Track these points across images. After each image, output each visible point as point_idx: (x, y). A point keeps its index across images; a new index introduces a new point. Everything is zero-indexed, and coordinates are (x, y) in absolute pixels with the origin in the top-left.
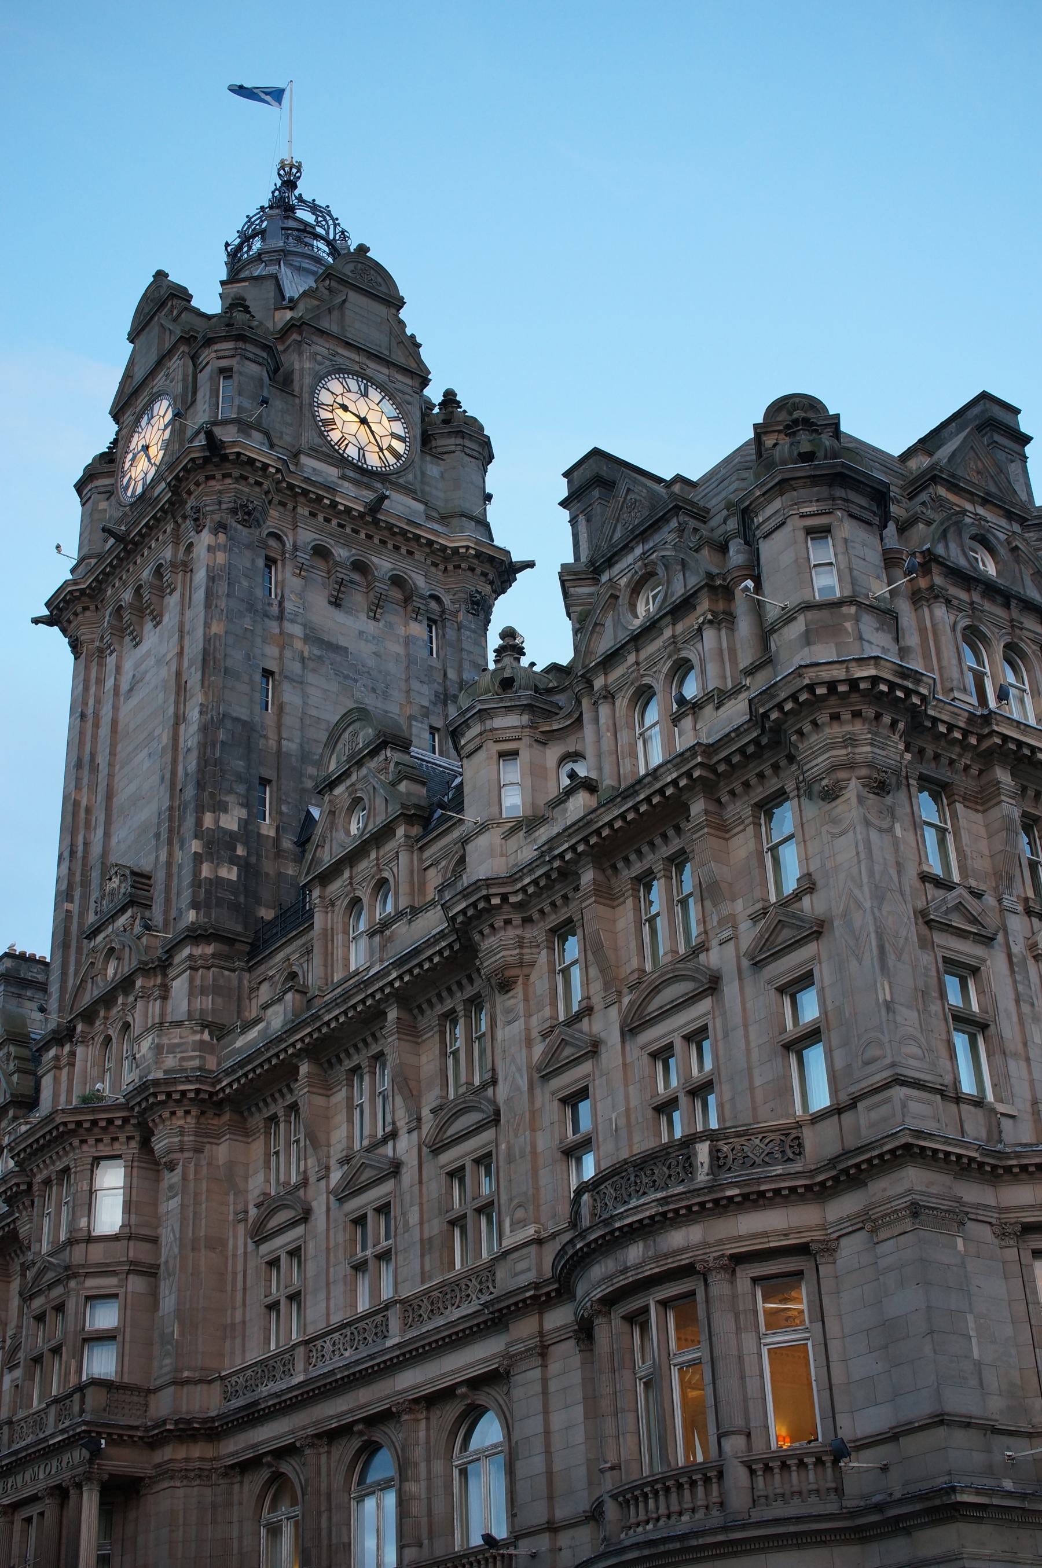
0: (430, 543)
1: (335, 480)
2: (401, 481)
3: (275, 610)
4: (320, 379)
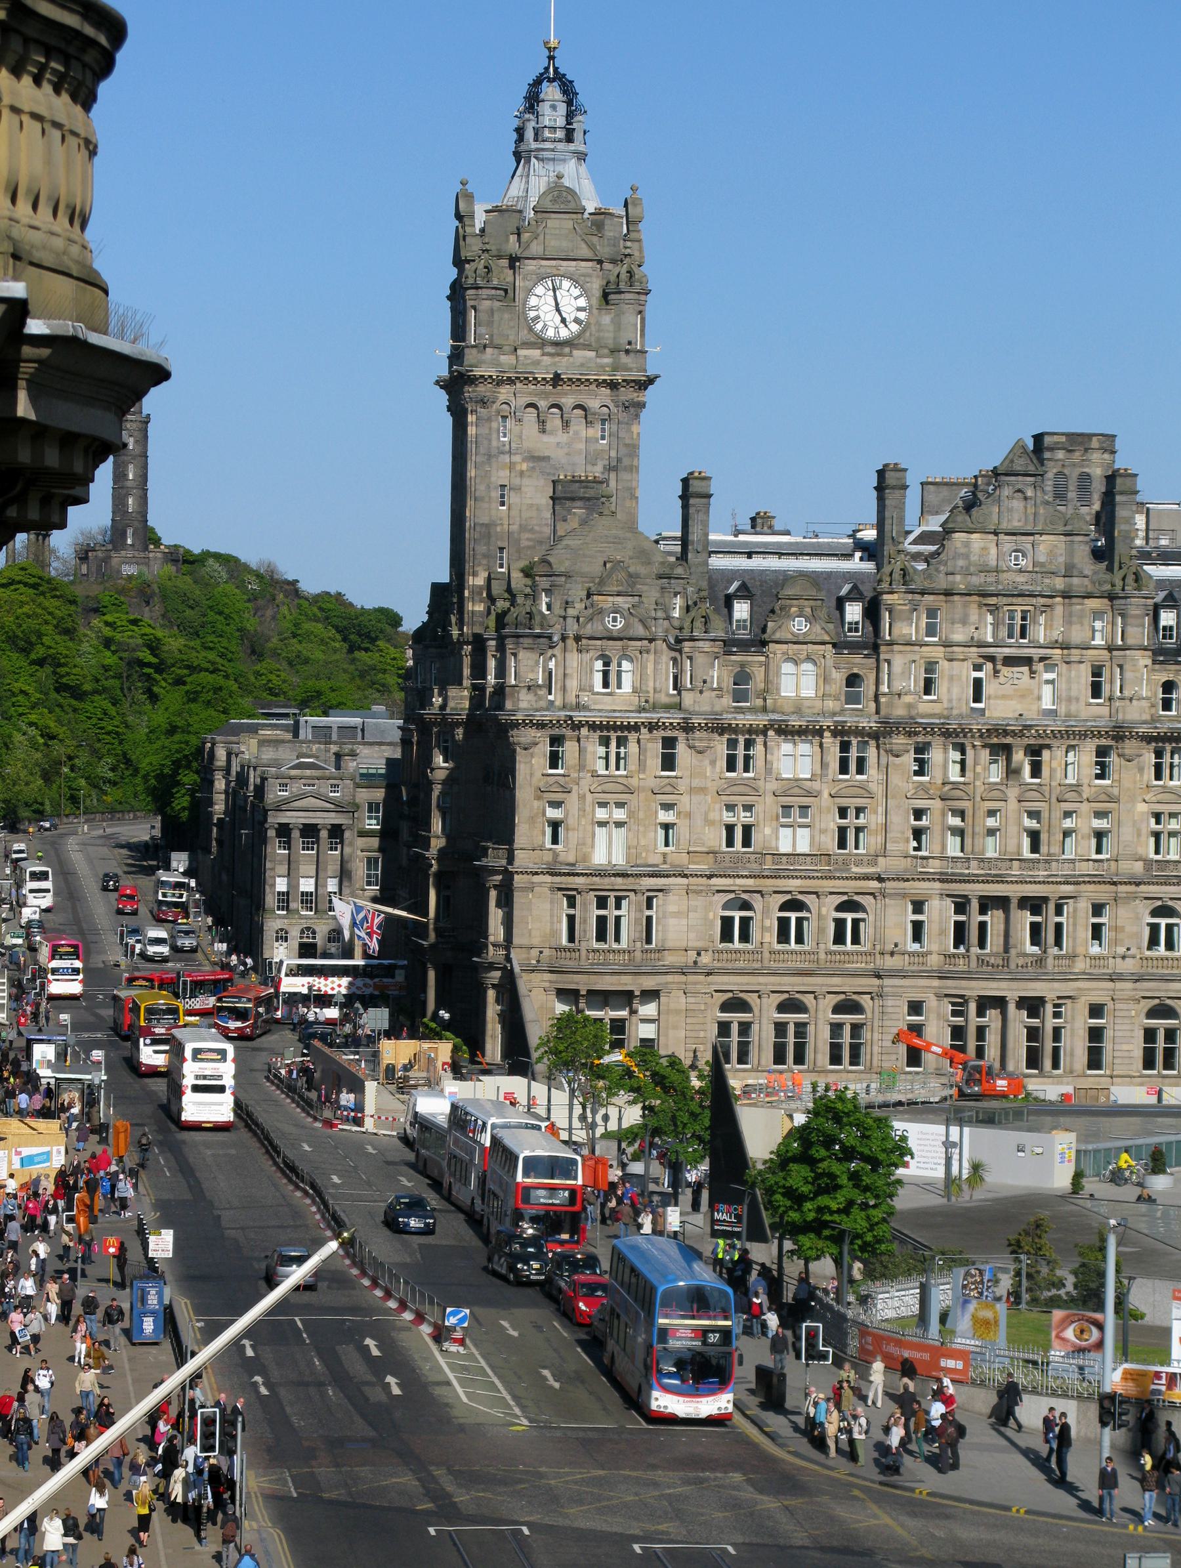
4: (529, 291)
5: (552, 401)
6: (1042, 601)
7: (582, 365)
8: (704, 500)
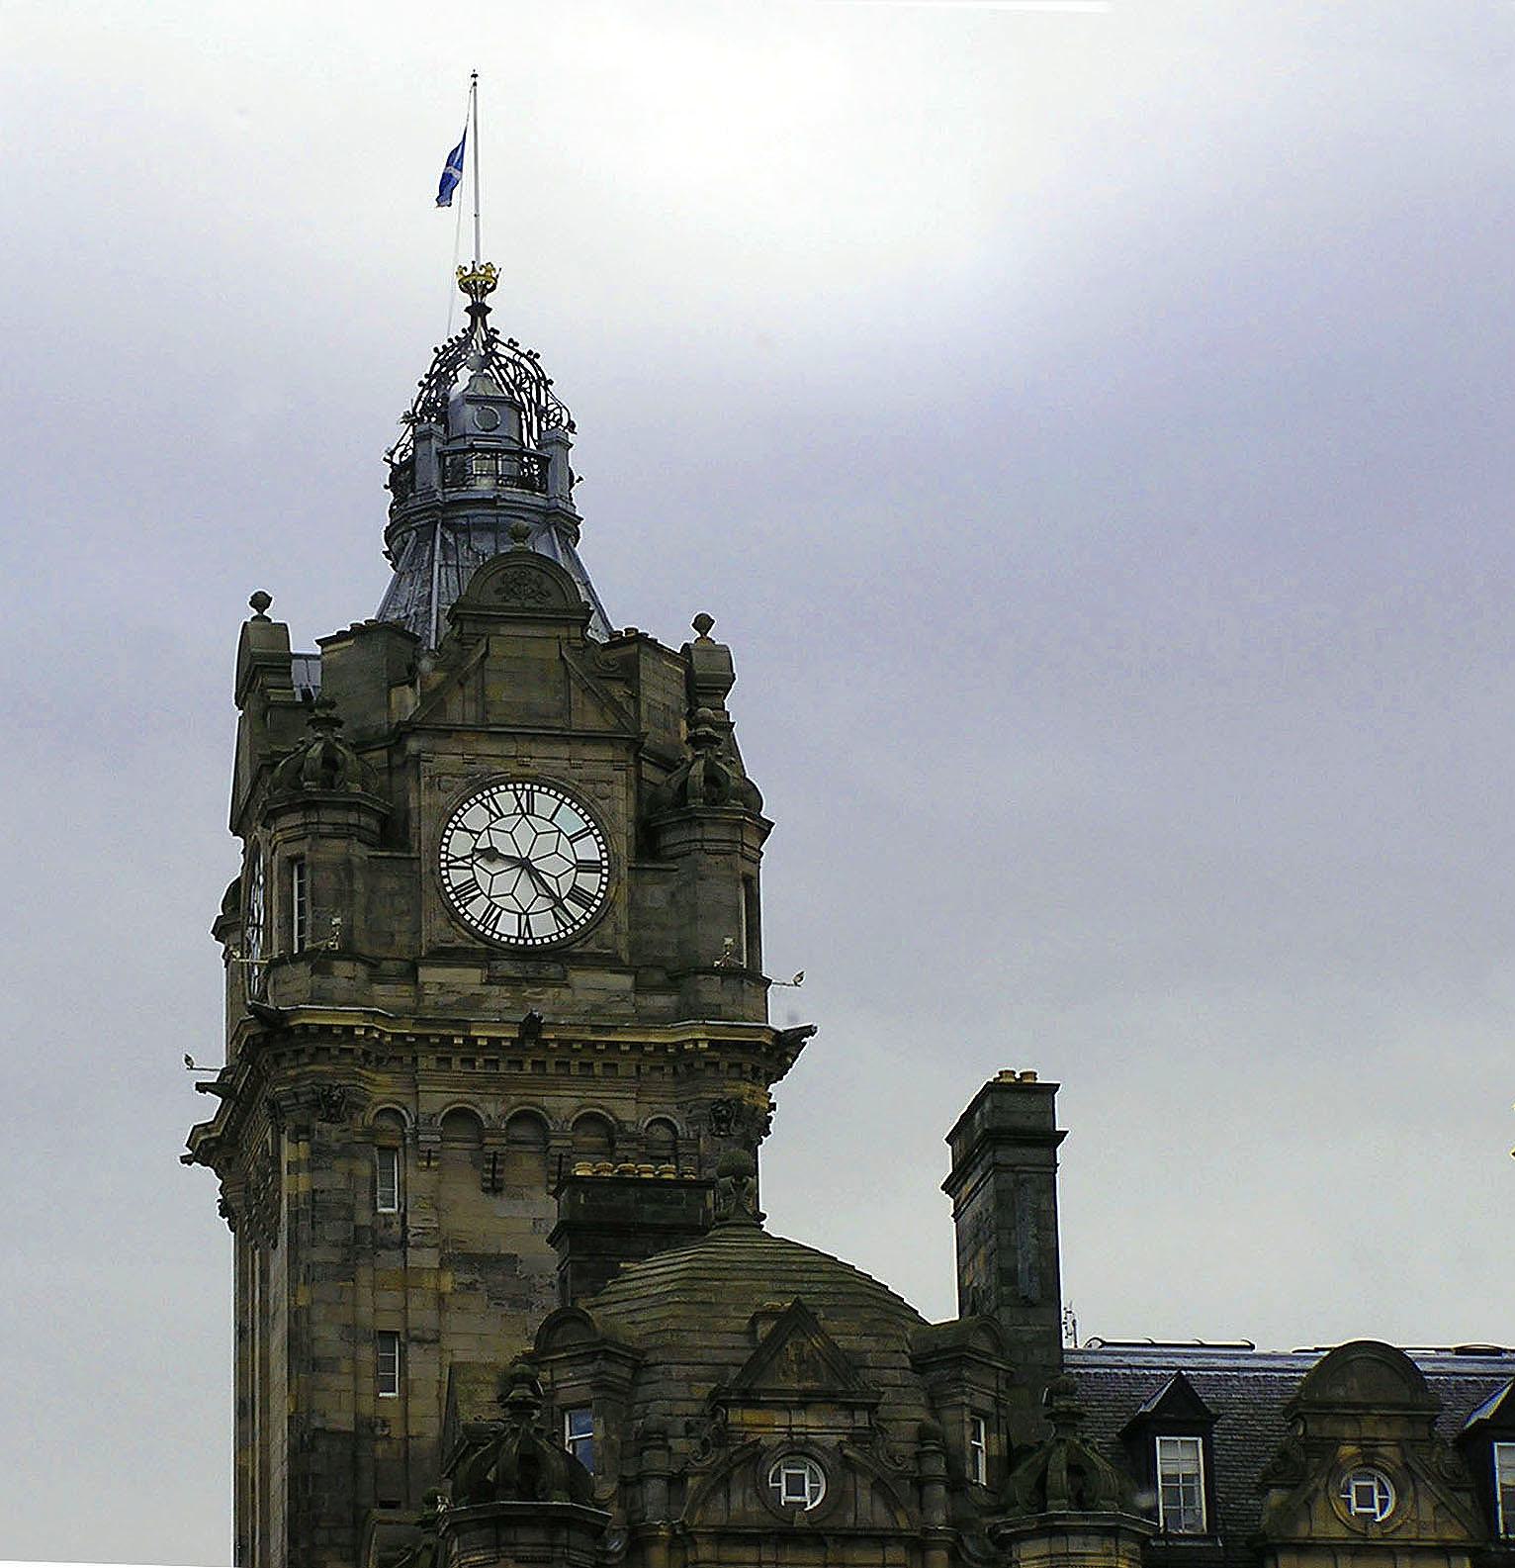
0: (637, 1047)
1: (478, 990)
2: (592, 946)
3: (397, 1228)
5: (515, 1101)
7: (596, 1009)
8: (1041, 1154)
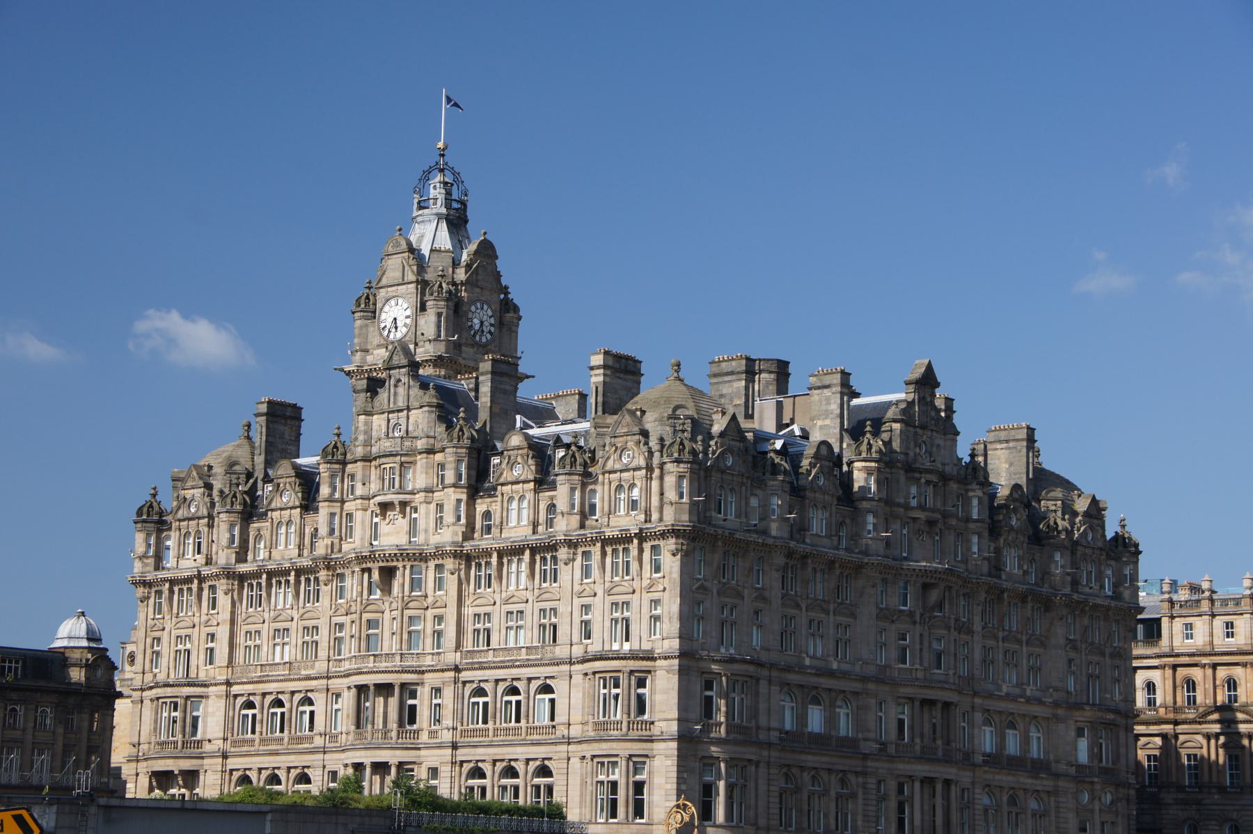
6: (403, 459)
